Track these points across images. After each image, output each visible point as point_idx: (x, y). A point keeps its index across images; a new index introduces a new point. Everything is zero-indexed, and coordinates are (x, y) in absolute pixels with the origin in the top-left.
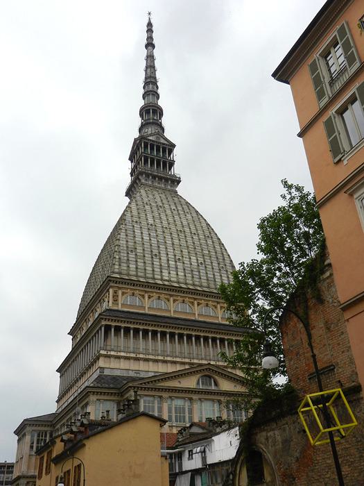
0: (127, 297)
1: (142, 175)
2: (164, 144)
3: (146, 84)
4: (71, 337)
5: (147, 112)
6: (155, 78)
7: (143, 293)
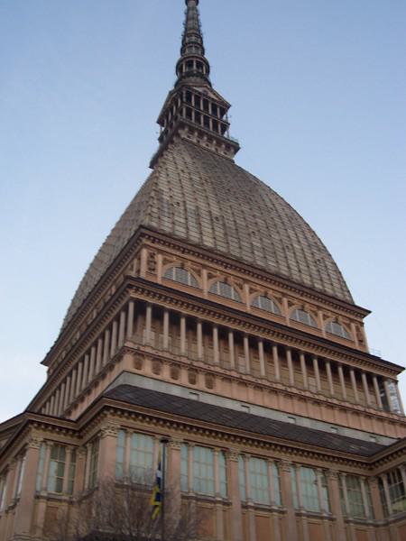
0: (170, 269)
1: (183, 128)
2: (213, 99)
3: (186, 35)
4: (46, 368)
5: (190, 64)
6: (199, 31)
7: (197, 268)
